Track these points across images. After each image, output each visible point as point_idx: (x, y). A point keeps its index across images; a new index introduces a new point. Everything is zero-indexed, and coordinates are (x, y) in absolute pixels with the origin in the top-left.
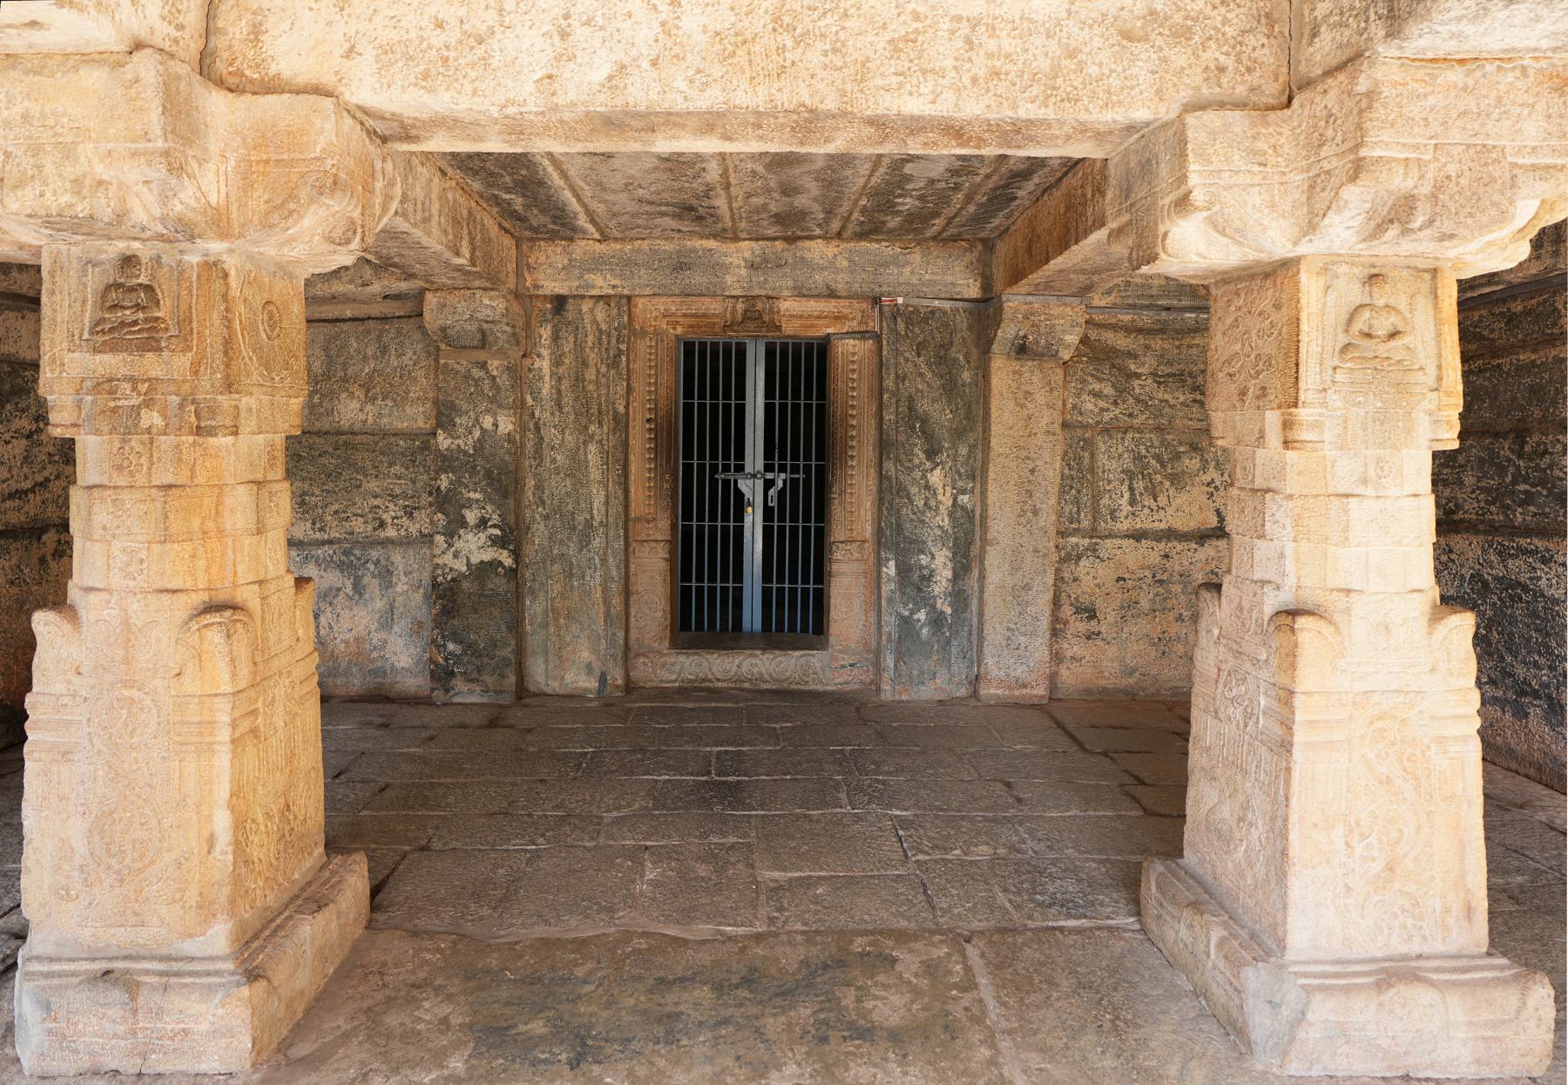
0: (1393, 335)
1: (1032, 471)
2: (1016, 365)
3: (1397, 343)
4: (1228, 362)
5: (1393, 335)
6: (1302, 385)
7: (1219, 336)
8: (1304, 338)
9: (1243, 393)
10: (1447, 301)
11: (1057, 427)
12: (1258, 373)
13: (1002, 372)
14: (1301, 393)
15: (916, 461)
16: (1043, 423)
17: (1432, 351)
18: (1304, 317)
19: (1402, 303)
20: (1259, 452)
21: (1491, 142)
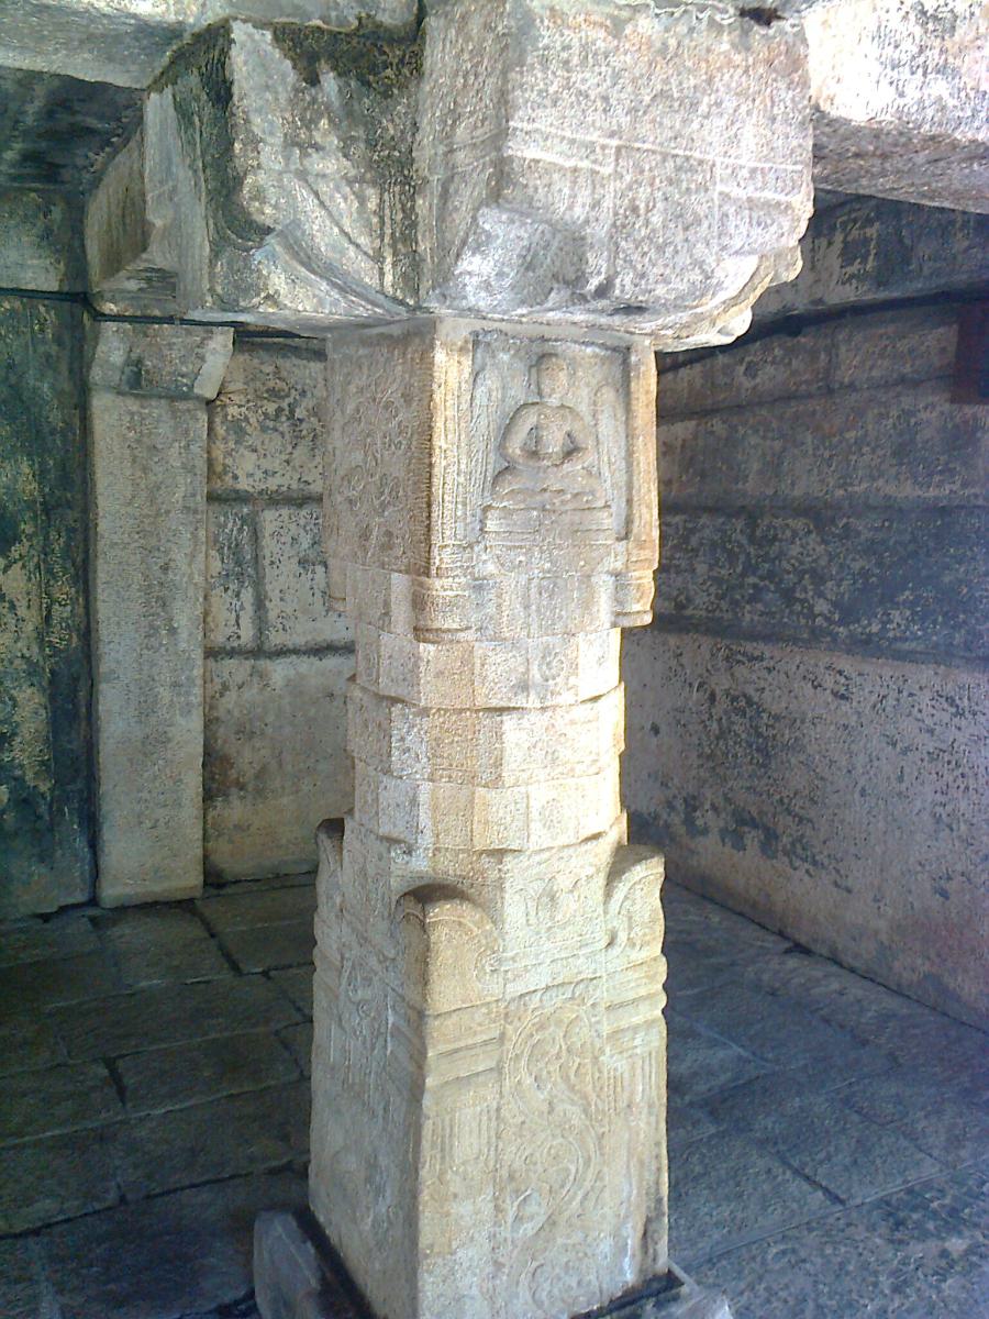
0: (571, 451)
1: (165, 568)
2: (133, 405)
3: (575, 467)
4: (347, 478)
5: (571, 451)
6: (436, 540)
7: (337, 434)
8: (439, 461)
9: (365, 535)
10: (643, 398)
11: (200, 499)
12: (384, 506)
13: (109, 414)
14: (435, 552)
16: (179, 495)
17: (622, 478)
18: (439, 424)
19: (581, 400)
20: (385, 638)
21: (697, 155)
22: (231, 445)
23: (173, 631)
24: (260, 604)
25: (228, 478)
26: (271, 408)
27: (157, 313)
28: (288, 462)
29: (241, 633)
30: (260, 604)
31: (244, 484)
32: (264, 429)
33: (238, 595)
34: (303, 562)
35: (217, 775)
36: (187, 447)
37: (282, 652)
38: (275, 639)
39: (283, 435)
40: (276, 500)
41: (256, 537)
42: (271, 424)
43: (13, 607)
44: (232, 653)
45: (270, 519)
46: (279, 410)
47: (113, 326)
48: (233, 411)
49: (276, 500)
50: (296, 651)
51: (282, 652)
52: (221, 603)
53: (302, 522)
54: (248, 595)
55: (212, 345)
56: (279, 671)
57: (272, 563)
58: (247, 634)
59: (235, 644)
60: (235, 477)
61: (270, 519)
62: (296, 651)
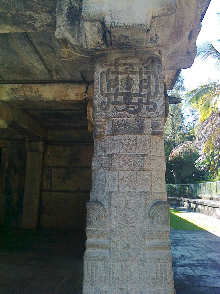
1: (35, 176)
15: (12, 174)
22: (48, 159)
23: (35, 186)
24: (51, 183)
25: (47, 164)
26: (54, 153)
27: (32, 140)
28: (56, 161)
29: (48, 187)
30: (51, 183)
31: (49, 165)
32: (53, 157)
33: (48, 182)
34: (58, 177)
35: (41, 210)
36: (39, 159)
37: (54, 191)
38: (53, 189)
39: (55, 157)
40: (55, 167)
41: (51, 172)
42: (54, 156)
43: (15, 181)
44: (47, 191)
45: (53, 170)
46: (55, 154)
47: (26, 142)
48: (48, 154)
49: (55, 167)
50: (56, 191)
51: (54, 191)
52: (45, 183)
53: (58, 171)
54: (49, 182)
55: (39, 144)
56: (54, 194)
57: (53, 177)
58: (49, 187)
59: (47, 189)
60: (48, 164)
61: (53, 170)
62: (56, 191)
